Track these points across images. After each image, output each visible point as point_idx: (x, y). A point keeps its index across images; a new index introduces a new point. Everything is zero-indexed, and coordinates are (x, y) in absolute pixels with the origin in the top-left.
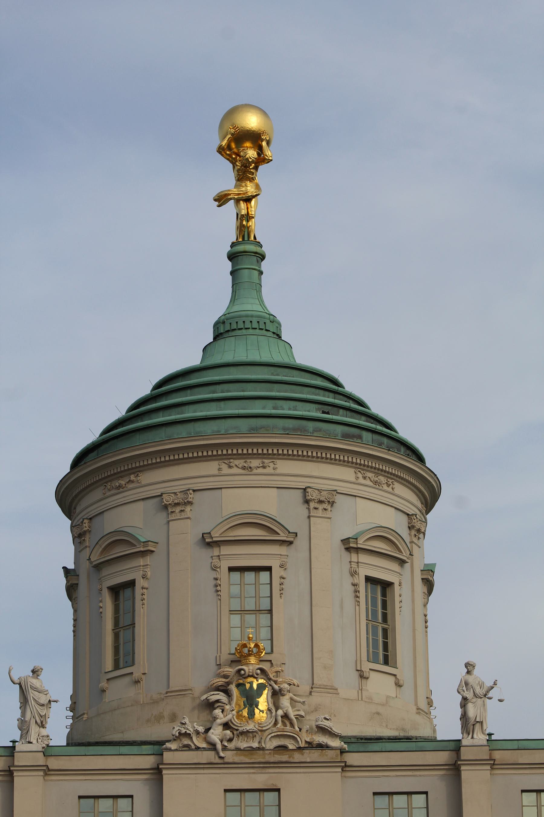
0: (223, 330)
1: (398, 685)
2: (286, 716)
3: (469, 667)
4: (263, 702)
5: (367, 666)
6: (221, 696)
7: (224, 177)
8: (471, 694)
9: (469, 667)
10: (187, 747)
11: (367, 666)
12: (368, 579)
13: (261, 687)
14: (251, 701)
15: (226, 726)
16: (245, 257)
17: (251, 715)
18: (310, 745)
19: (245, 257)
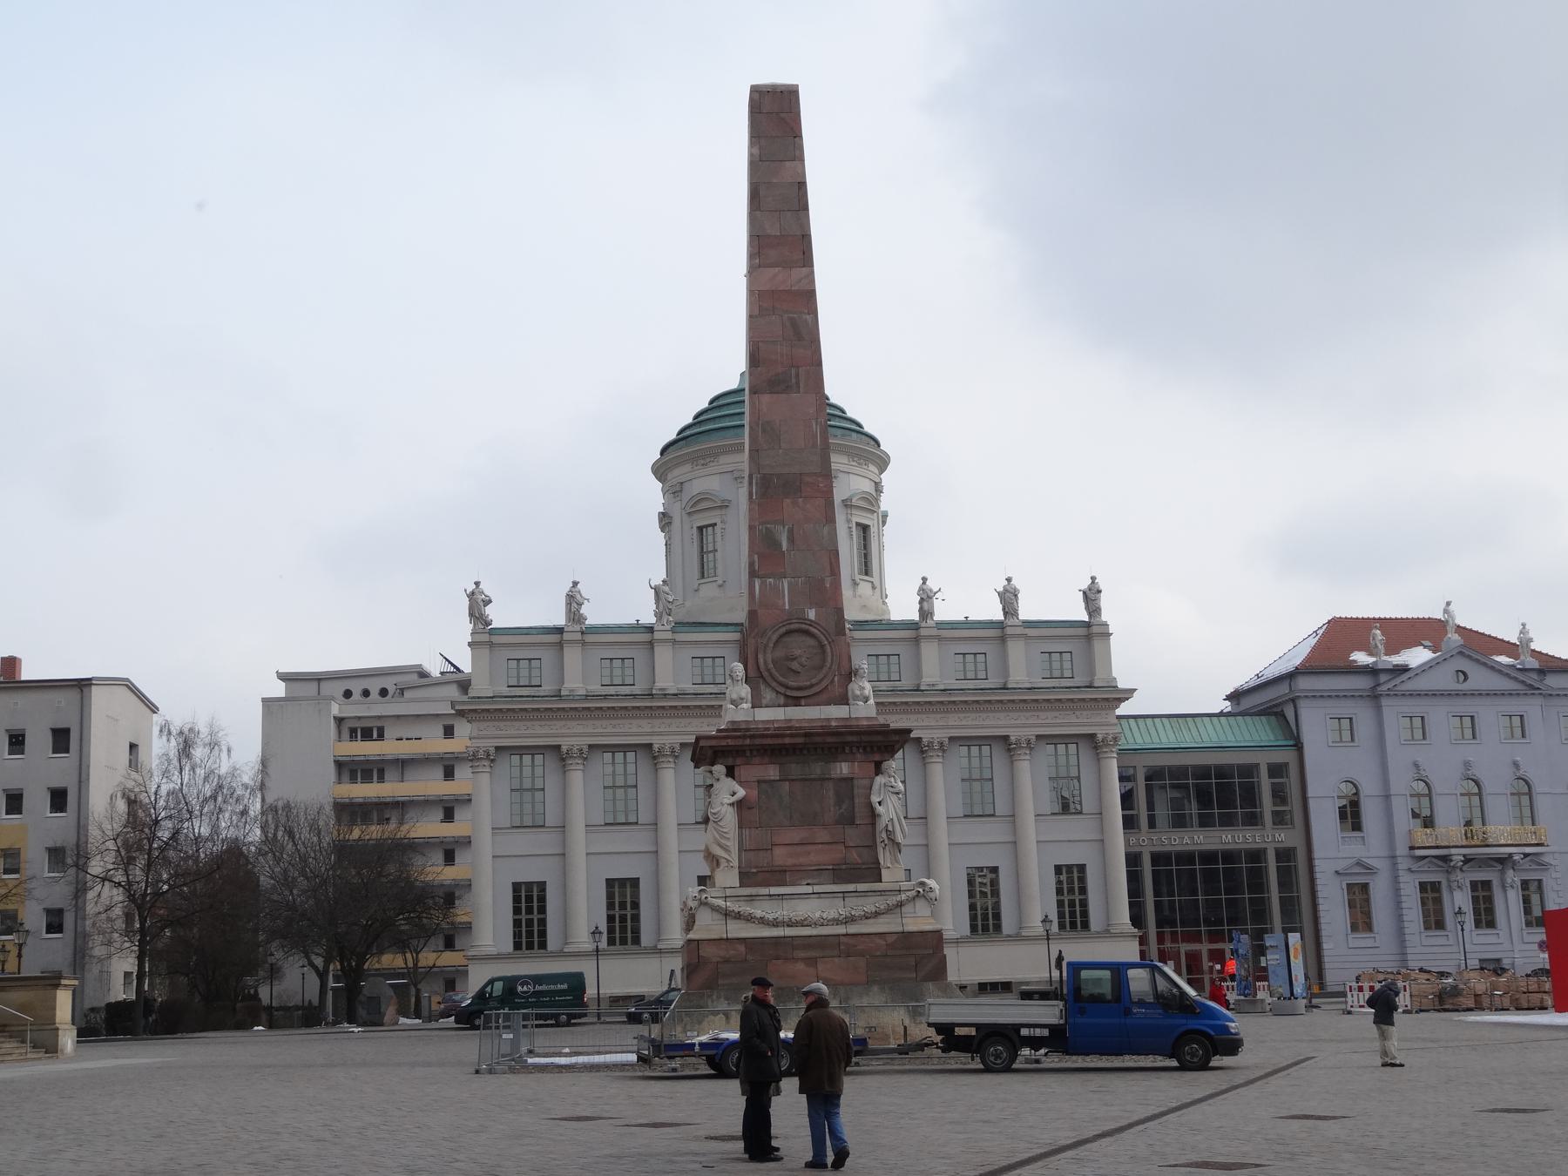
1: (874, 588)
3: (924, 580)
5: (858, 577)
8: (926, 598)
11: (858, 577)
12: (858, 524)
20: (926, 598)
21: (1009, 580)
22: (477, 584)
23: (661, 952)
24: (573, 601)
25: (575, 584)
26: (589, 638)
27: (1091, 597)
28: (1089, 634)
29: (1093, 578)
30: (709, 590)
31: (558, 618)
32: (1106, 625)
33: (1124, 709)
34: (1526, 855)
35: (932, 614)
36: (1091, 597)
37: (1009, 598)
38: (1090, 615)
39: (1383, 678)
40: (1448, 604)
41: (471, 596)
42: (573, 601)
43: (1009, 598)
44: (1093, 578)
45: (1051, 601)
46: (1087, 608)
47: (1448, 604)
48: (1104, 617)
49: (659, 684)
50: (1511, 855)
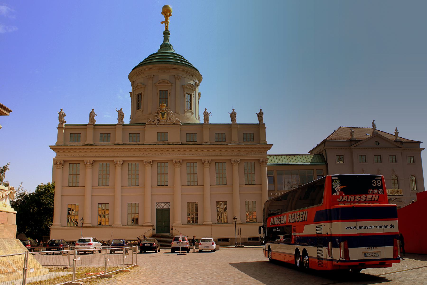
0: (162, 47)
2: (170, 119)
3: (206, 109)
4: (165, 115)
6: (157, 114)
7: (163, 18)
8: (206, 115)
9: (206, 109)
10: (150, 124)
13: (165, 113)
14: (163, 115)
15: (158, 120)
16: (166, 34)
17: (163, 118)
18: (174, 124)
19: (166, 34)
20: (206, 115)
21: (233, 110)
22: (61, 110)
23: (113, 227)
24: (92, 115)
25: (93, 110)
26: (96, 127)
27: (260, 115)
28: (260, 127)
29: (261, 110)
30: (139, 113)
31: (86, 121)
32: (264, 124)
33: (269, 152)
34: (396, 199)
35: (208, 120)
36: (260, 115)
37: (233, 116)
38: (259, 121)
39: (353, 143)
40: (374, 121)
41: (60, 114)
42: (92, 115)
43: (233, 116)
44: (261, 110)
45: (247, 117)
46: (259, 119)
47: (374, 121)
48: (264, 122)
49: (117, 141)
50: (391, 199)
